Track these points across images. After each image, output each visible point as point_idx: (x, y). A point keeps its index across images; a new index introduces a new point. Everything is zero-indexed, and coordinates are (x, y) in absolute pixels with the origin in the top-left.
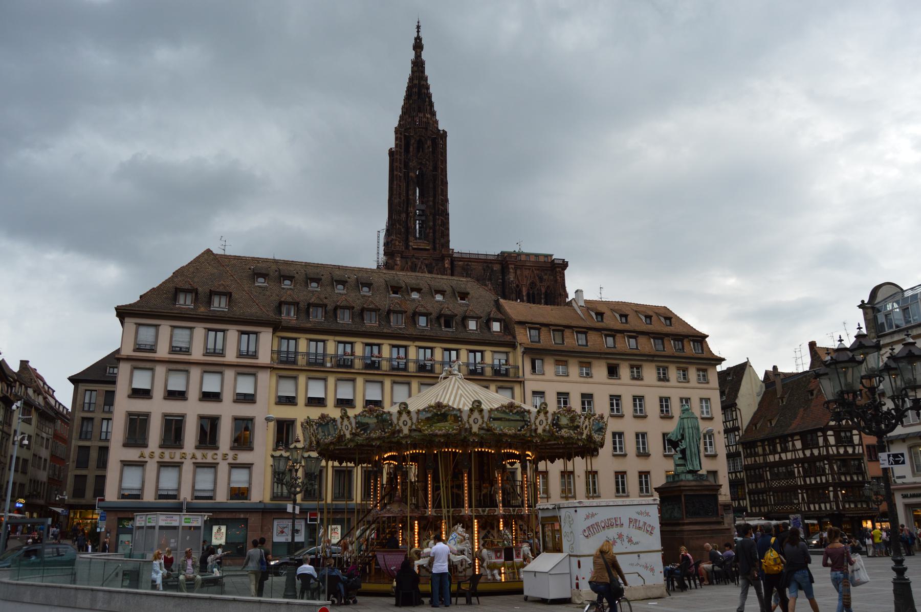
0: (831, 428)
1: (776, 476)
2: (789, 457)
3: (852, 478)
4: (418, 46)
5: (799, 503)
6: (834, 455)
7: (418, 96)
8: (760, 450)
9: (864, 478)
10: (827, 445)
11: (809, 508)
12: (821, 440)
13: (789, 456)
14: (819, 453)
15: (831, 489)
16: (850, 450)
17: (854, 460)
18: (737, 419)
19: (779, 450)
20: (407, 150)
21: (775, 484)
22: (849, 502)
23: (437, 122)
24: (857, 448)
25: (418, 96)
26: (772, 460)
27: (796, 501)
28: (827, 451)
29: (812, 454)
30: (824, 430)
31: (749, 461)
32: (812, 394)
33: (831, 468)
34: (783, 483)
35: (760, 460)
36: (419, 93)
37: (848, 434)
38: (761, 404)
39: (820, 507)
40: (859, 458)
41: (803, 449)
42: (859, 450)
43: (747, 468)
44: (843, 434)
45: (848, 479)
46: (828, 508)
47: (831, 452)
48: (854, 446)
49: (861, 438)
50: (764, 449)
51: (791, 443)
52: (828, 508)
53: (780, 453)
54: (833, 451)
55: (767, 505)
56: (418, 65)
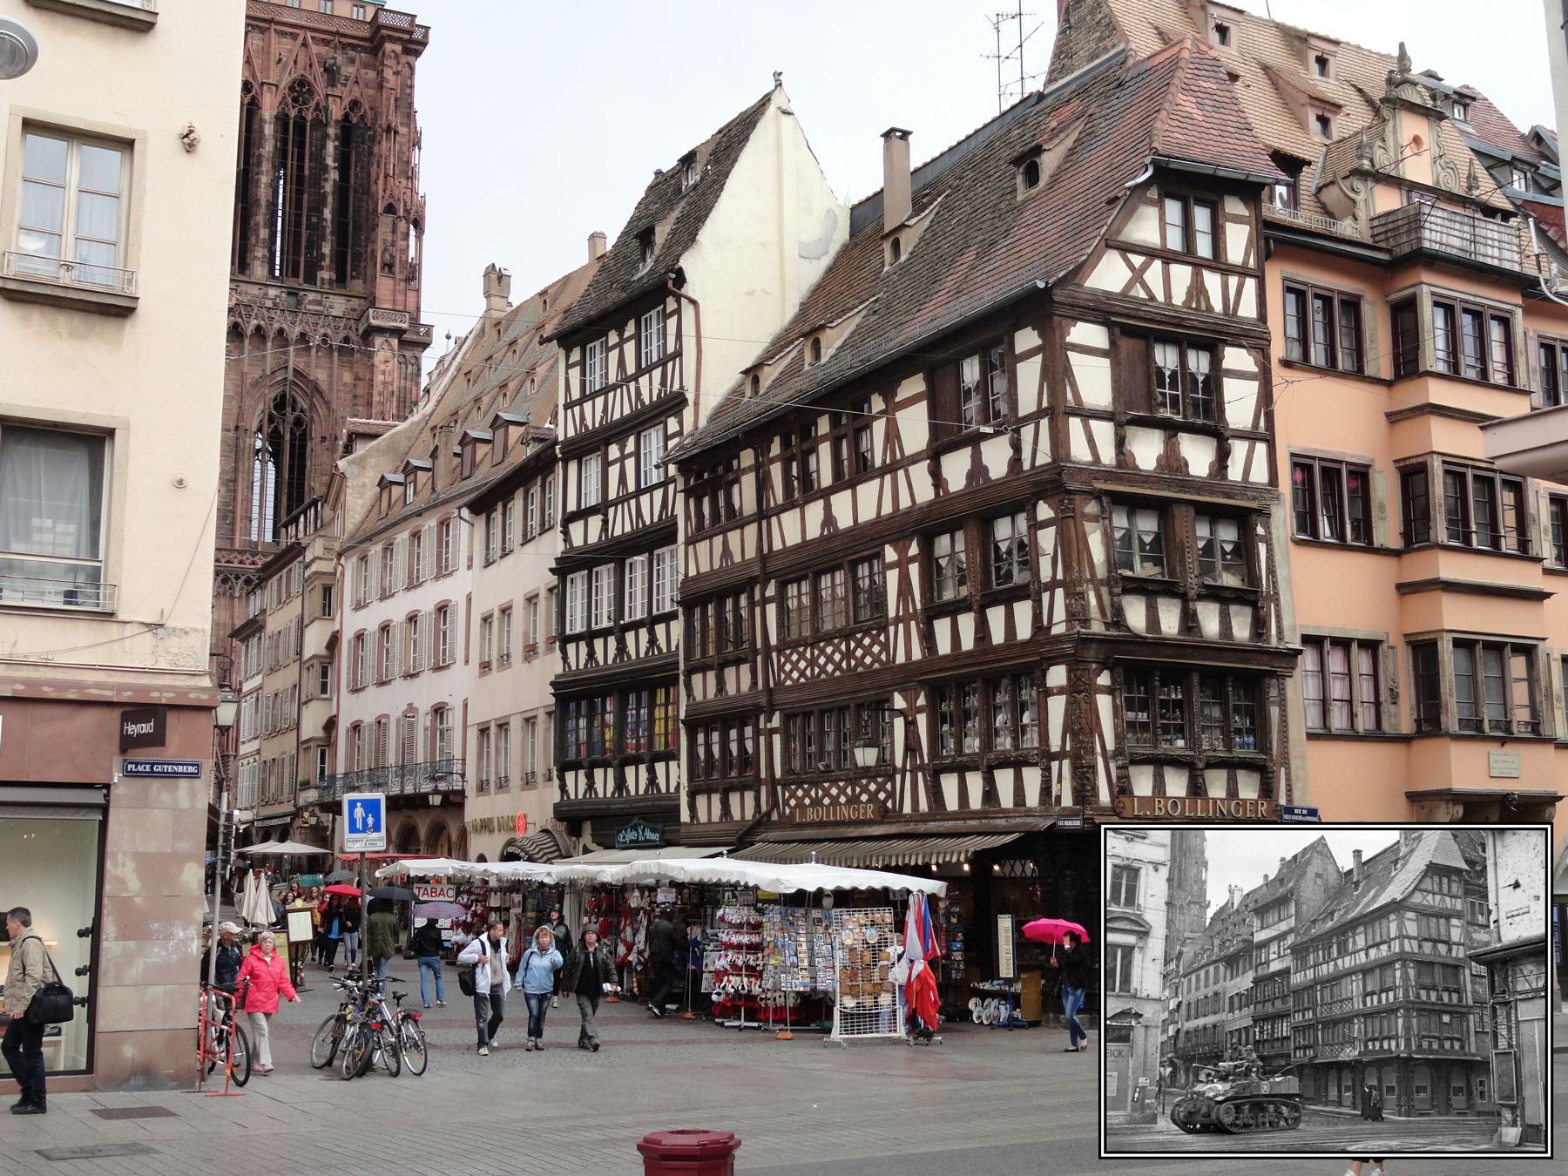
0: (1101, 310)
2: (867, 514)
3: (1189, 621)
5: (884, 769)
6: (1095, 471)
8: (745, 495)
9: (1259, 625)
10: (1060, 408)
11: (936, 794)
12: (1029, 374)
13: (865, 504)
14: (1016, 462)
15: (1057, 676)
16: (1198, 456)
17: (1215, 514)
18: (678, 354)
19: (826, 479)
21: (795, 669)
22: (1160, 763)
24: (1239, 449)
26: (793, 538)
27: (866, 756)
28: (1059, 441)
29: (978, 470)
30: (1042, 307)
31: (704, 558)
32: (1032, 176)
33: (1073, 548)
34: (831, 660)
35: (743, 544)
37: (1199, 363)
39: (990, 794)
40: (1245, 517)
41: (935, 454)
42: (1248, 465)
43: (695, 597)
44: (1166, 358)
45: (1170, 622)
46: (1032, 798)
47: (1079, 451)
48: (1220, 436)
49: (1266, 399)
50: (763, 485)
51: (879, 427)
52: (1032, 798)
53: (825, 494)
54: (1093, 443)
55: (754, 785)
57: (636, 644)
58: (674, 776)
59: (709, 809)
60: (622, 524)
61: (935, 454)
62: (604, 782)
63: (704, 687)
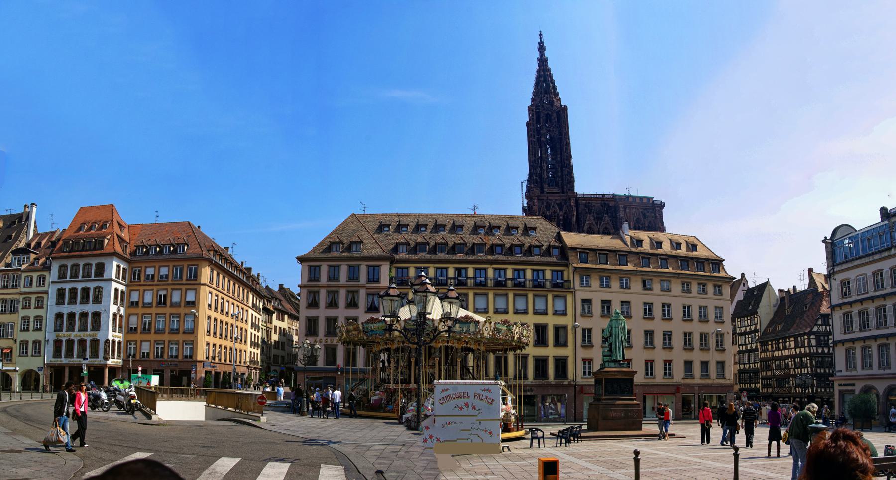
0: (814, 333)
1: (779, 367)
4: (541, 48)
6: (814, 353)
7: (544, 84)
10: (810, 346)
12: (806, 341)
13: (787, 352)
20: (538, 122)
21: (777, 372)
23: (559, 100)
25: (544, 84)
31: (763, 355)
33: (811, 362)
34: (782, 372)
35: (769, 354)
36: (545, 81)
38: (776, 314)
41: (795, 348)
43: (761, 360)
54: (813, 350)
56: (543, 62)
57: (752, 366)
58: (759, 385)
59: (765, 390)
60: (749, 348)
61: (795, 348)
62: (747, 386)
63: (764, 373)
